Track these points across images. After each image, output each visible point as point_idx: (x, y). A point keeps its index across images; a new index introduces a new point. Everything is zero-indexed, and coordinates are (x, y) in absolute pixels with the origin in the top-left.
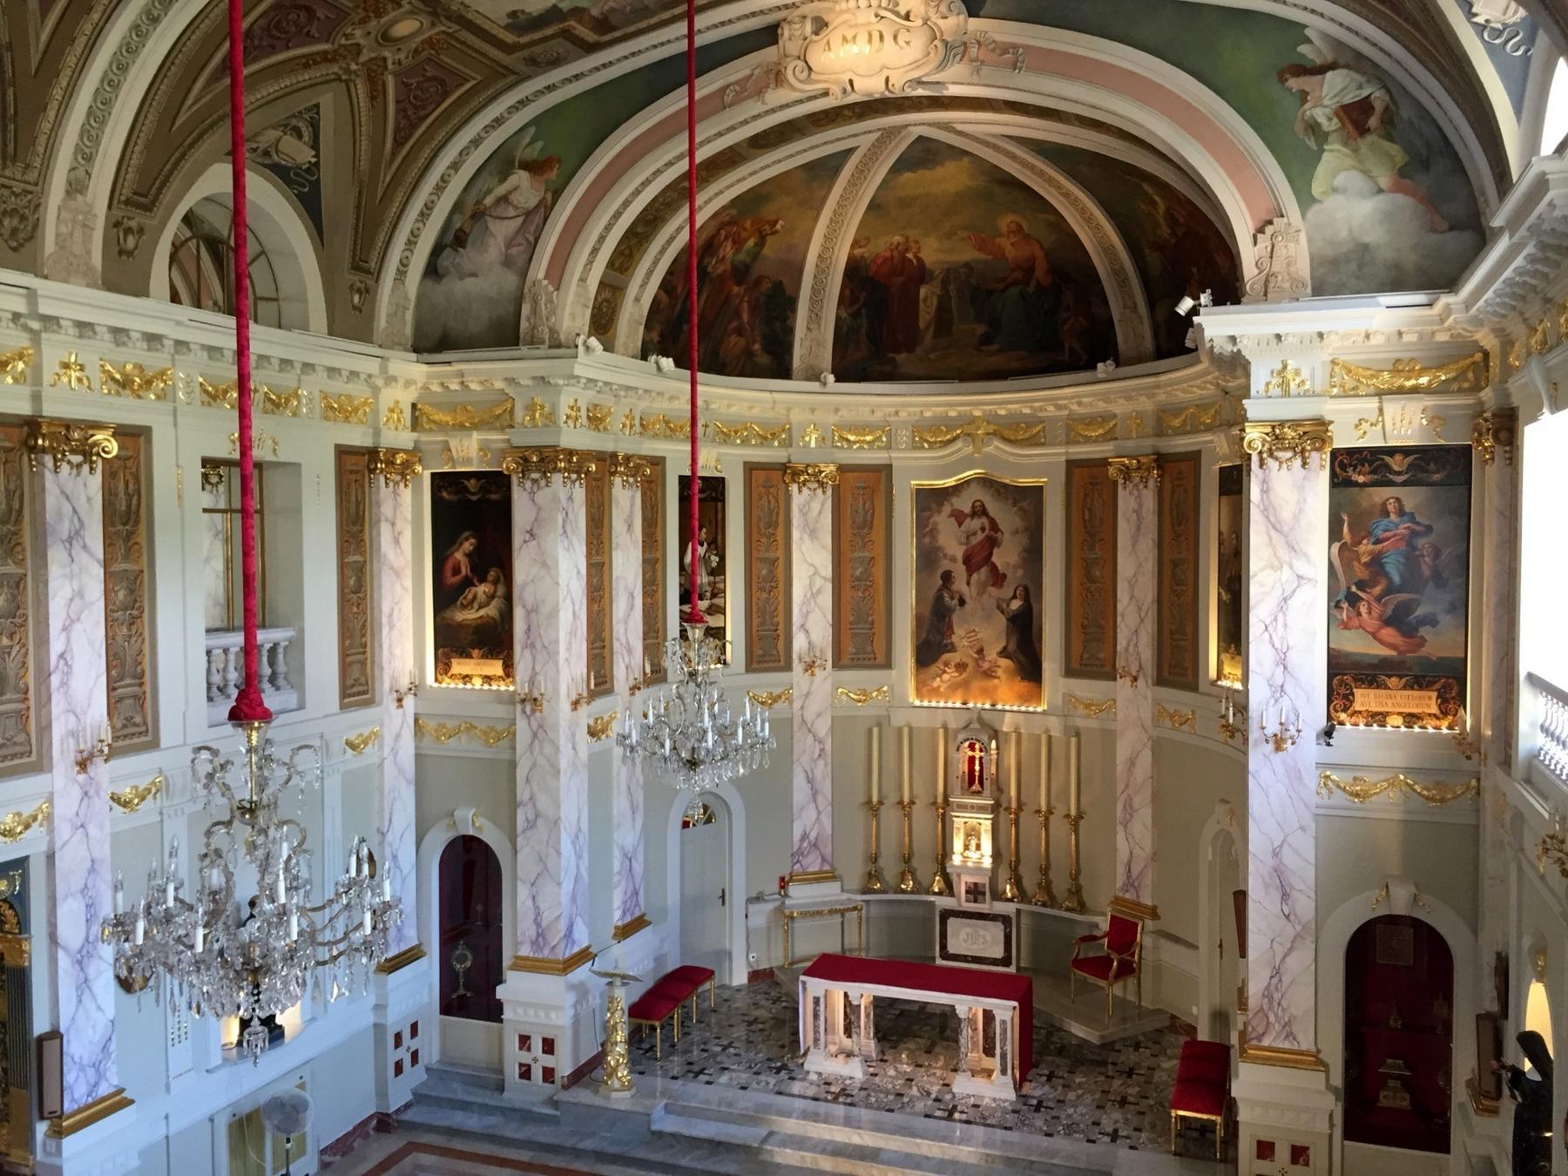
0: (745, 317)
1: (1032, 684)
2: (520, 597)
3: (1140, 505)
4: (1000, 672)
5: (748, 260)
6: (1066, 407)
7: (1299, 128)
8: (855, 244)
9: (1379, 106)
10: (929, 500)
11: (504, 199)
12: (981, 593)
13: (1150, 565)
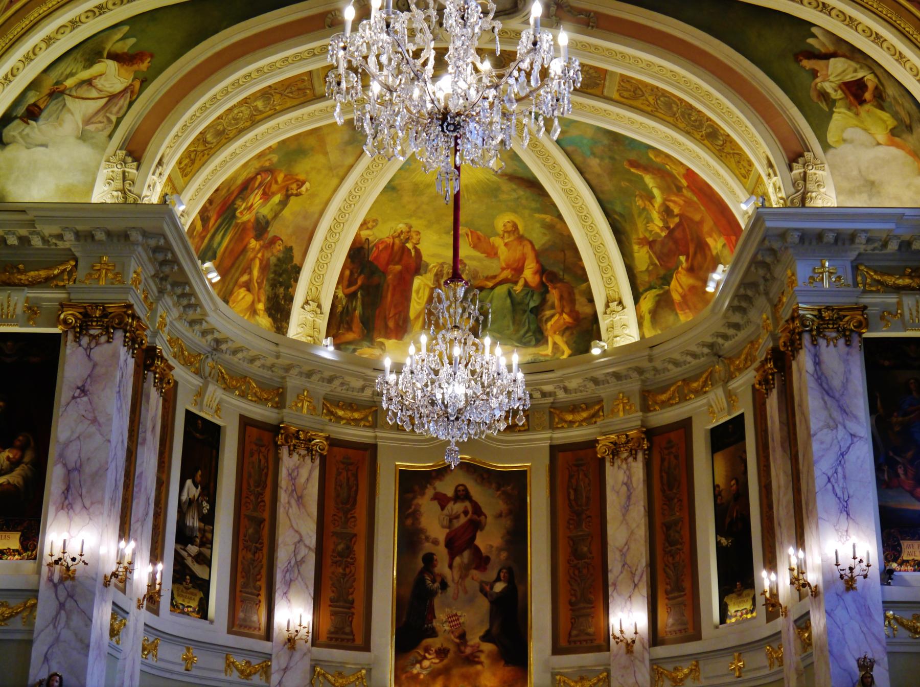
0: (256, 273)
2: (61, 456)
3: (630, 477)
4: (483, 658)
5: (269, 217)
6: (550, 394)
7: (813, 95)
8: (364, 225)
9: (871, 86)
10: (411, 483)
11: (89, 82)
12: (463, 577)
13: (642, 532)
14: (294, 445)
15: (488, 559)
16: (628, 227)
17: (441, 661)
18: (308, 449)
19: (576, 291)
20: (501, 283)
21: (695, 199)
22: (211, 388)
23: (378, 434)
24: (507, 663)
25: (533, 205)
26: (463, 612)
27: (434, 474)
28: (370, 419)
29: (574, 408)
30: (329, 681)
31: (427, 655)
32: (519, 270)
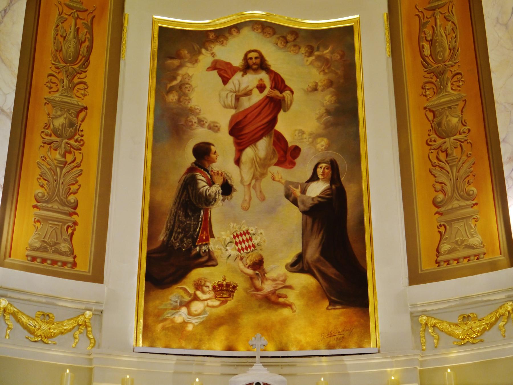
1: (350, 311)
4: (292, 297)
12: (257, 177)
15: (296, 150)
17: (223, 303)
24: (332, 303)
26: (259, 223)
27: (212, 36)
30: (25, 327)
31: (199, 293)
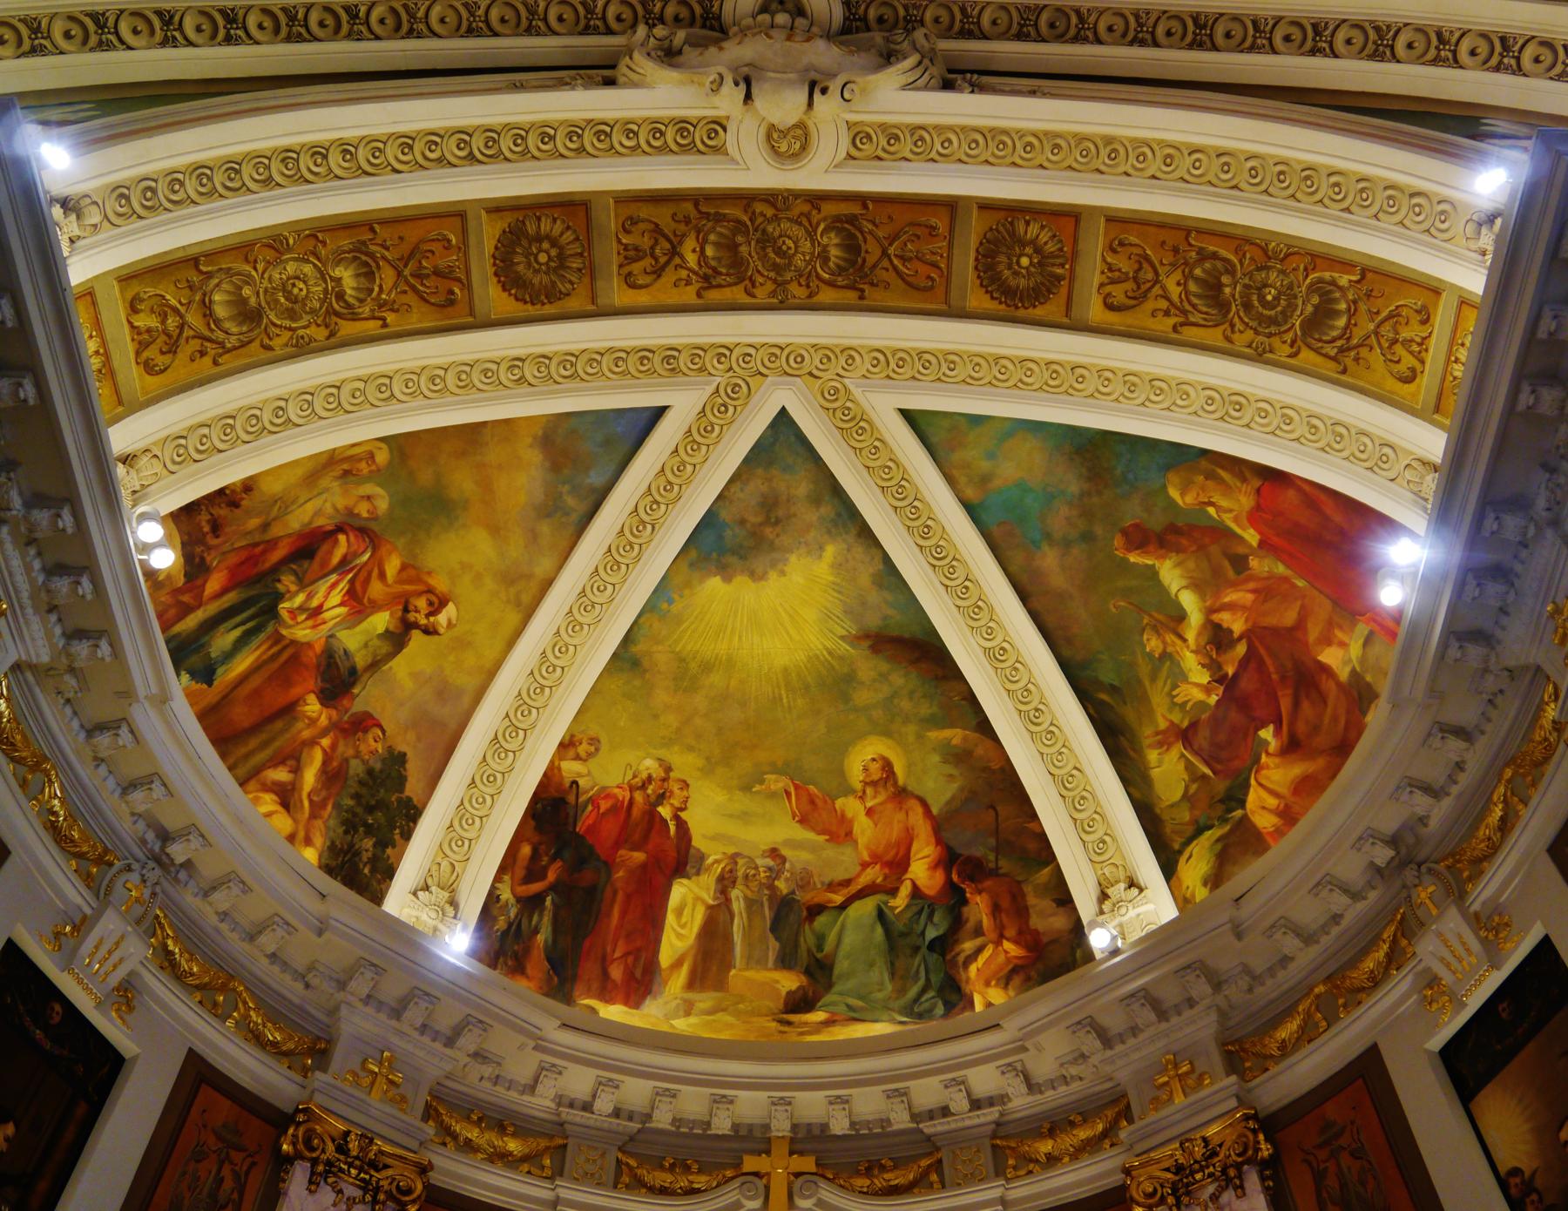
5: (360, 661)
14: (329, 1163)
16: (1129, 713)
18: (365, 1186)
19: (1028, 889)
20: (861, 894)
21: (1281, 569)
22: (110, 924)
23: (564, 1194)
25: (926, 709)
28: (547, 1162)
29: (1053, 1124)
32: (899, 865)
